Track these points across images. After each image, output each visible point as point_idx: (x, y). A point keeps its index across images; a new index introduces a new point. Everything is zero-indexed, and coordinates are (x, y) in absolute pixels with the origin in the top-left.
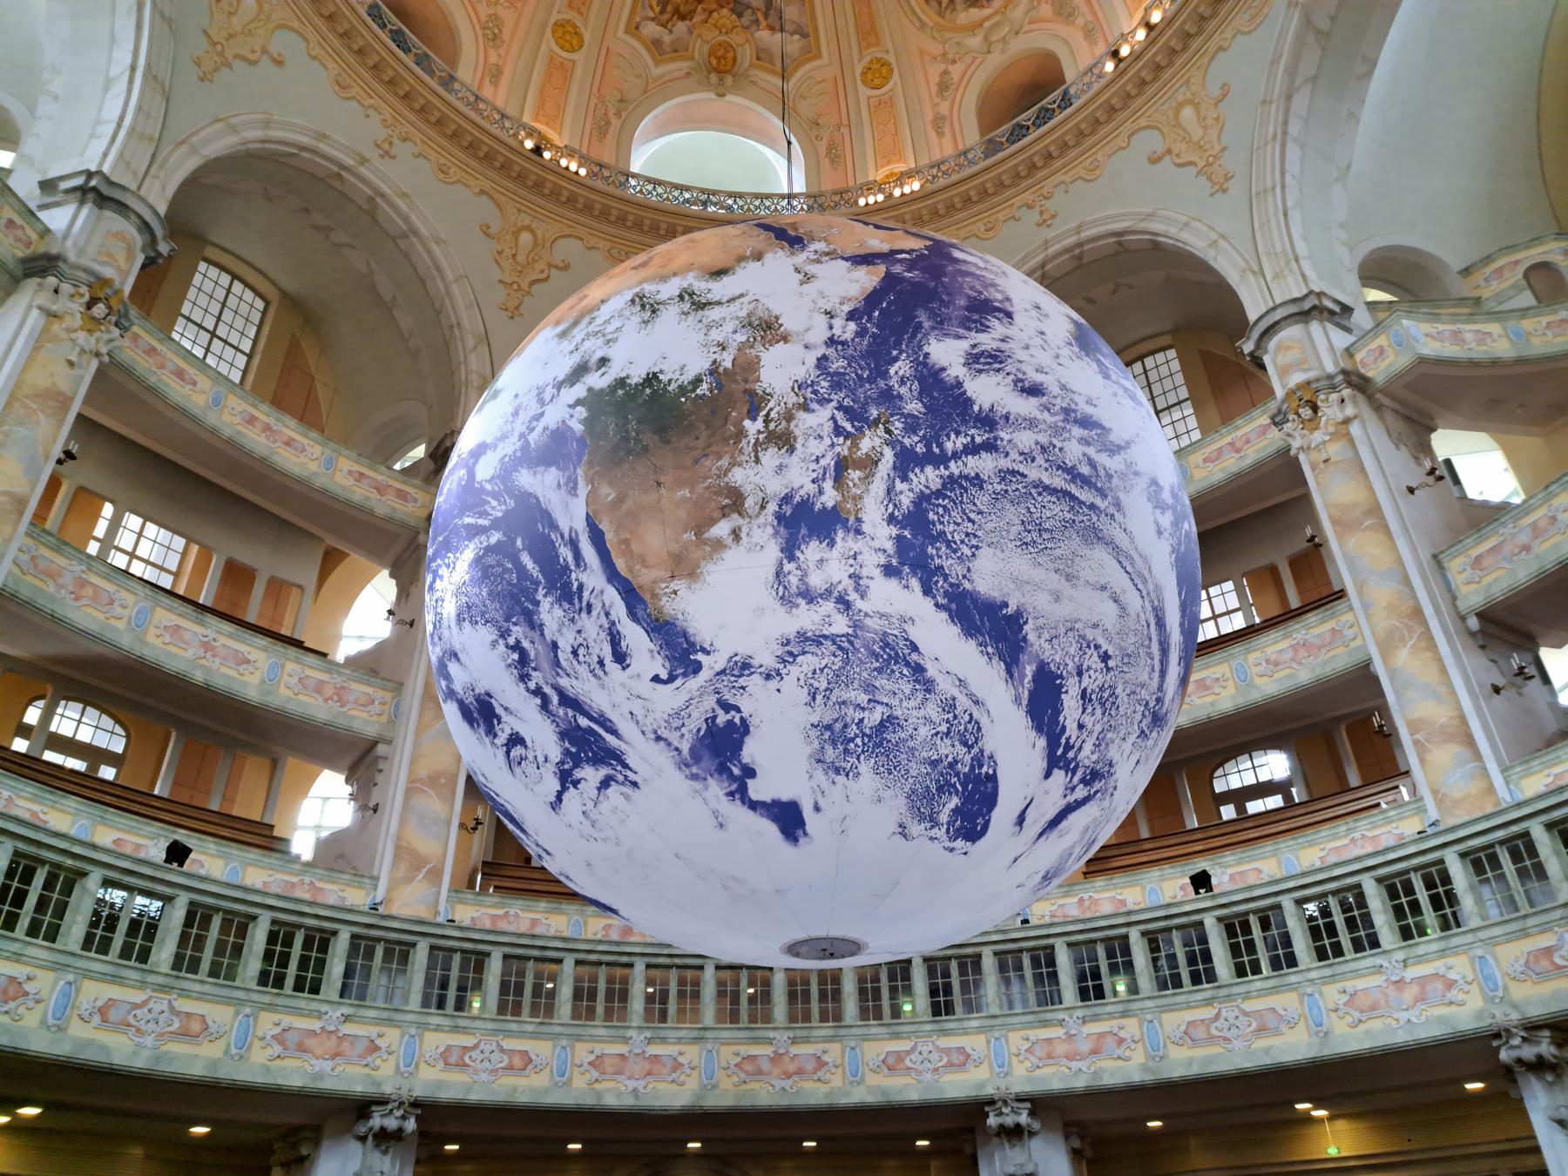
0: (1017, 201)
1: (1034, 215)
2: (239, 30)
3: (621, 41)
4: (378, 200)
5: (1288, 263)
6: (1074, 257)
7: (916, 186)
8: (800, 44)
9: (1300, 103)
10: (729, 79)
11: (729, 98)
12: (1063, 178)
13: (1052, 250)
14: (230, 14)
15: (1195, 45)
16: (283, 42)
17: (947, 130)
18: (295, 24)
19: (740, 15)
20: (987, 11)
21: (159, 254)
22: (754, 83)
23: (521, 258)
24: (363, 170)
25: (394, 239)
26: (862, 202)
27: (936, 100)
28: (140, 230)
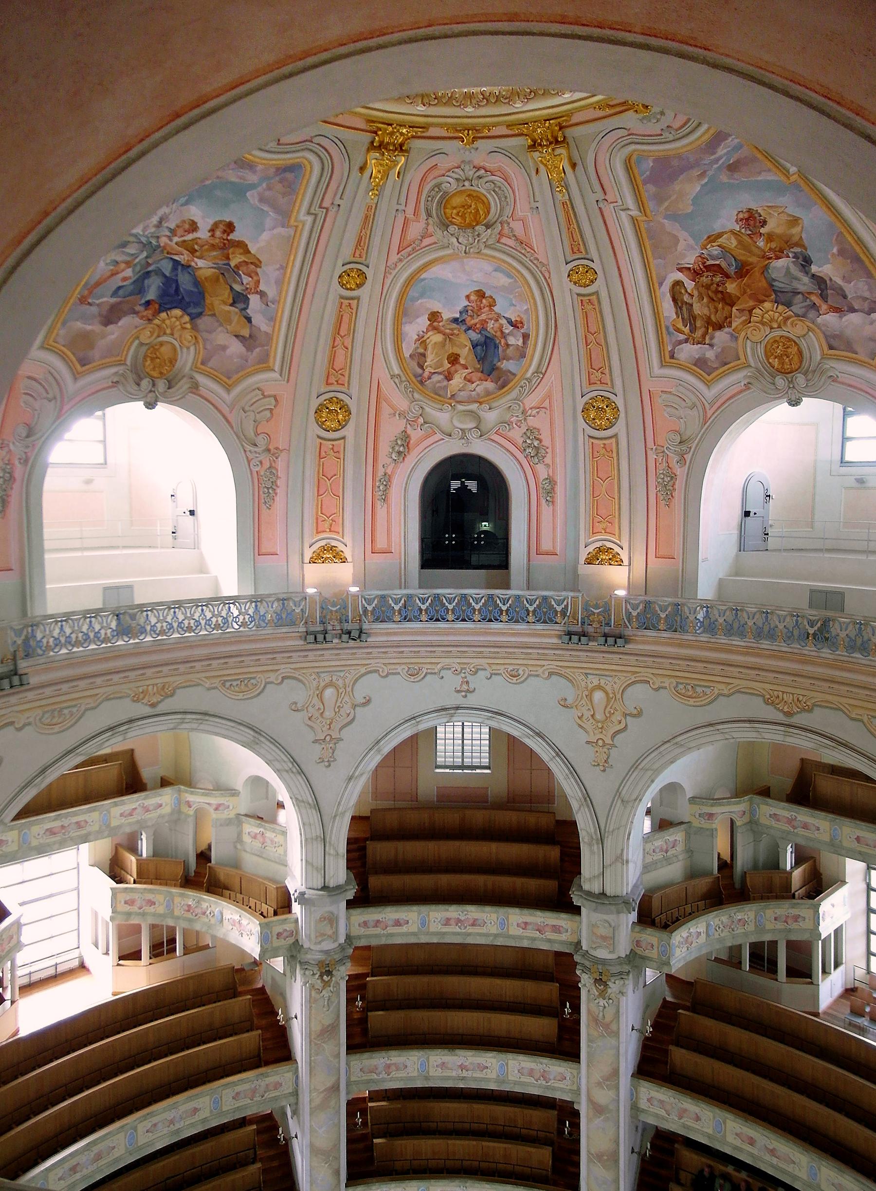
10: (800, 379)
19: (788, 305)
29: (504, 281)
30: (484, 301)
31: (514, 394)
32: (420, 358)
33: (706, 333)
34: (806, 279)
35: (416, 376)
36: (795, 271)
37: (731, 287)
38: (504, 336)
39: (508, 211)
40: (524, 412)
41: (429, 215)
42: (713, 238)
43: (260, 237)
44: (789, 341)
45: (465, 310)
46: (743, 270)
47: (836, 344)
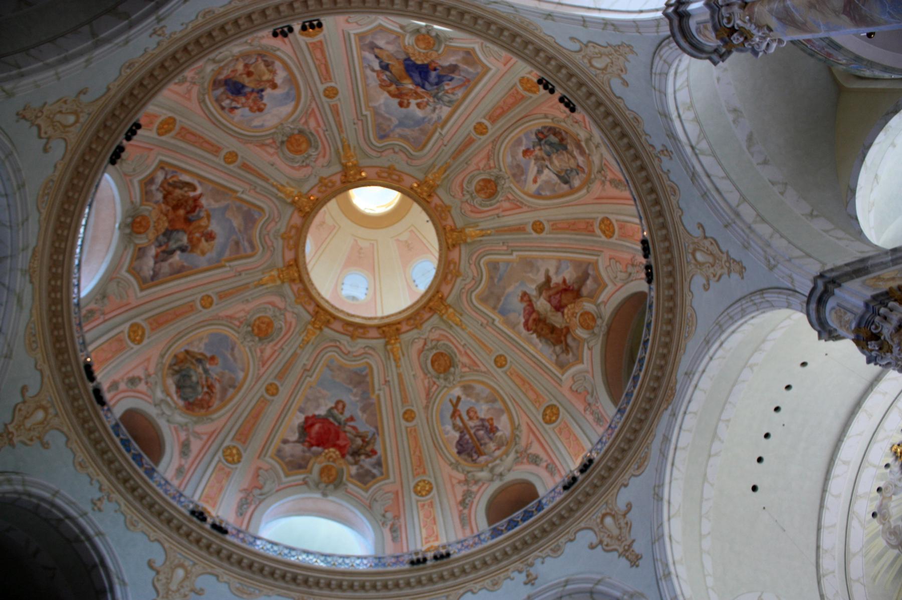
0: (102, 478)
4: (126, 22)
10: (128, 231)
12: (123, 505)
13: (81, 521)
15: (214, 559)
19: (164, 234)
20: (175, 397)
23: (58, 117)
24: (153, 18)
27: (125, 380)
30: (255, 108)
31: (206, 85)
32: (268, 64)
33: (164, 189)
34: (174, 246)
35: (265, 56)
36: (179, 244)
37: (181, 212)
38: (233, 100)
41: (311, 133)
42: (209, 217)
43: (383, 99)
44: (147, 228)
45: (262, 98)
47: (140, 253)
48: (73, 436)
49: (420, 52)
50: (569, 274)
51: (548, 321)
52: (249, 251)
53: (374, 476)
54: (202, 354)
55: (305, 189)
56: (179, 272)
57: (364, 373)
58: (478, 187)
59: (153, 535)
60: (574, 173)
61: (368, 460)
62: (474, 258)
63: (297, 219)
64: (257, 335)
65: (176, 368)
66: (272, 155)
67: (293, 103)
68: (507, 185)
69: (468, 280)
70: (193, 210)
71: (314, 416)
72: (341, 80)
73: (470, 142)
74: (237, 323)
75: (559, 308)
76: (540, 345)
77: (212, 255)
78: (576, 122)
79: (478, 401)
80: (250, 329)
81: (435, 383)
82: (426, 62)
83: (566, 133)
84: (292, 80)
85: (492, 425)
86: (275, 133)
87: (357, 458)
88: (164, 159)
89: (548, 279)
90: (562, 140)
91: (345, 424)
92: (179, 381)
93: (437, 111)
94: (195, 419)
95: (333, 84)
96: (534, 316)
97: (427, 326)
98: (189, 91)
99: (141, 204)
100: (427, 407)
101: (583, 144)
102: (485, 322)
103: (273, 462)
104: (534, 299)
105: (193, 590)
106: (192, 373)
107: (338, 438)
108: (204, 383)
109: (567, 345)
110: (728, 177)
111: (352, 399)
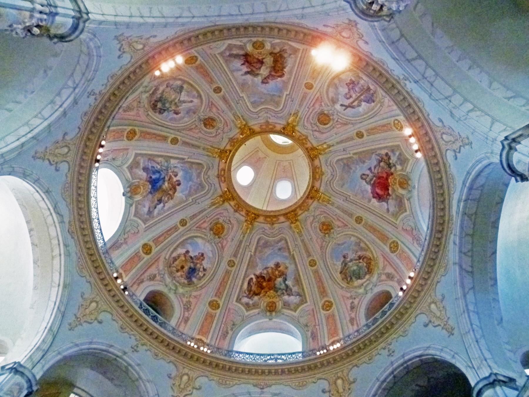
1: (385, 352)
2: (88, 313)
3: (234, 304)
4: (130, 368)
5: (481, 362)
6: (405, 368)
7: (338, 345)
8: (299, 299)
9: (470, 297)
10: (274, 313)
11: (274, 320)
12: (395, 336)
13: (395, 366)
14: (86, 309)
16: (104, 316)
17: (355, 323)
18: (109, 310)
19: (277, 292)
21: (33, 391)
22: (283, 314)
23: (182, 386)
25: (133, 381)
26: (318, 353)
27: (350, 313)
28: (27, 382)
29: (211, 255)
30: (202, 258)
31: (191, 288)
32: (175, 259)
34: (284, 285)
35: (170, 264)
36: (282, 282)
37: (264, 284)
38: (199, 270)
39: (226, 237)
40: (190, 296)
41: (211, 223)
43: (179, 194)
45: (195, 256)
46: (270, 280)
47: (286, 305)
48: (355, 362)
49: (144, 189)
50: (237, 64)
51: (273, 65)
52: (283, 242)
53: (400, 154)
54: (342, 264)
55: (243, 219)
56: (298, 281)
57: (342, 164)
58: (211, 127)
59: (413, 320)
60: (172, 87)
61: (392, 158)
62: (255, 116)
63: (261, 219)
64: (330, 230)
65: (349, 279)
66: (227, 241)
67: (195, 239)
68: (202, 114)
69: (269, 115)
70: (263, 278)
71: (372, 193)
72: (175, 220)
73: (185, 143)
74: (324, 243)
75: (261, 62)
76: (289, 65)
77: (287, 262)
78: (140, 102)
79: (338, 94)
80: (327, 235)
81: (337, 121)
82: (148, 183)
83: (150, 102)
84: (182, 244)
85: (350, 84)
86: (214, 243)
87: (392, 165)
88: (235, 299)
89: (247, 73)
90: (156, 101)
91: (374, 173)
92: (356, 278)
93: (176, 165)
94: (376, 269)
95: (178, 224)
96: (273, 73)
97: (304, 132)
98: (195, 297)
99: (260, 308)
100: (352, 124)
101: (151, 92)
102: (290, 99)
103: (399, 219)
104: (264, 76)
105: (442, 301)
106: (352, 269)
107: (383, 177)
108: (357, 261)
109: (280, 51)
110: (78, 62)
111: (360, 170)
